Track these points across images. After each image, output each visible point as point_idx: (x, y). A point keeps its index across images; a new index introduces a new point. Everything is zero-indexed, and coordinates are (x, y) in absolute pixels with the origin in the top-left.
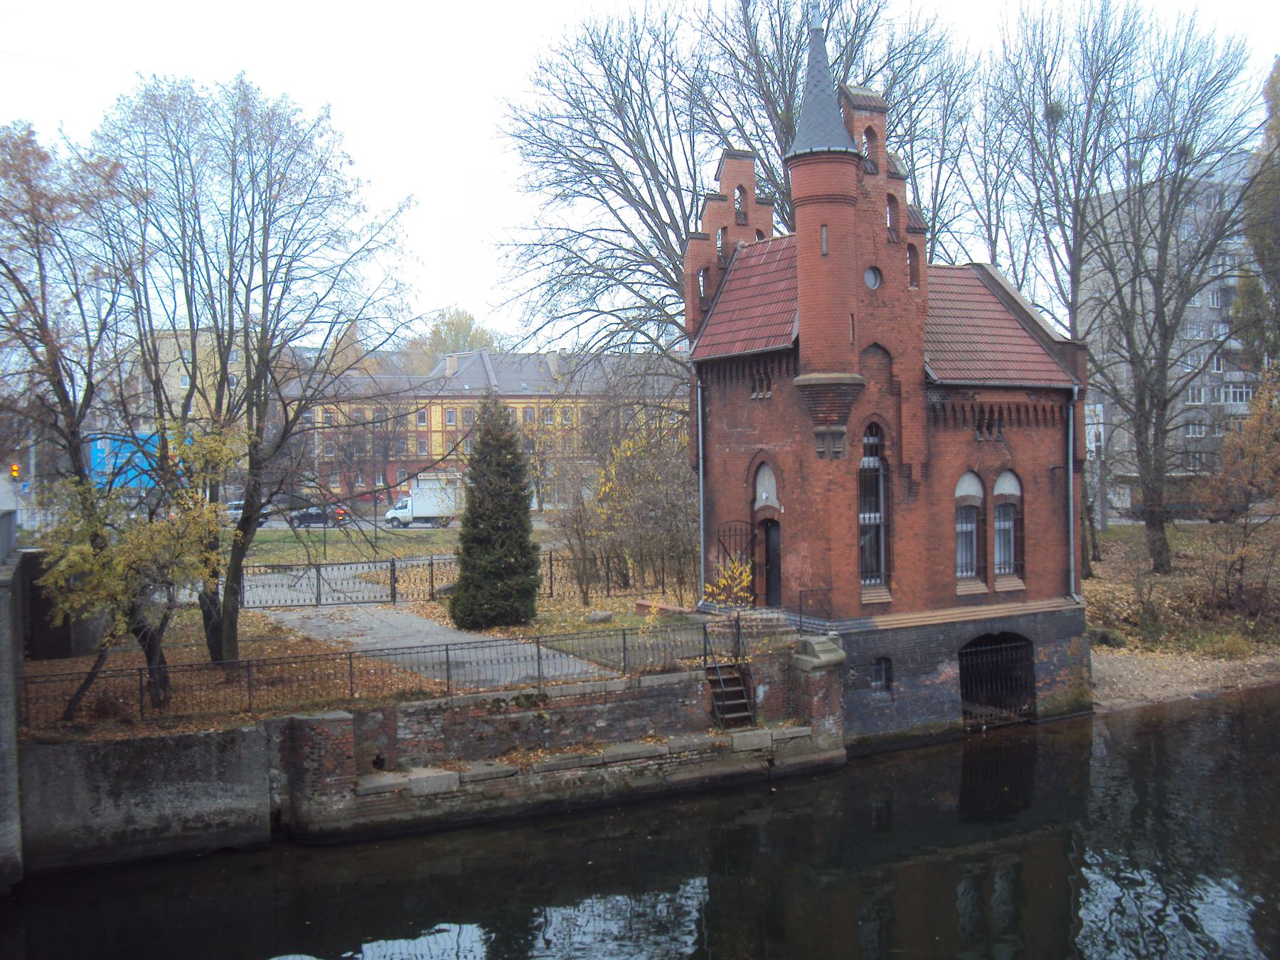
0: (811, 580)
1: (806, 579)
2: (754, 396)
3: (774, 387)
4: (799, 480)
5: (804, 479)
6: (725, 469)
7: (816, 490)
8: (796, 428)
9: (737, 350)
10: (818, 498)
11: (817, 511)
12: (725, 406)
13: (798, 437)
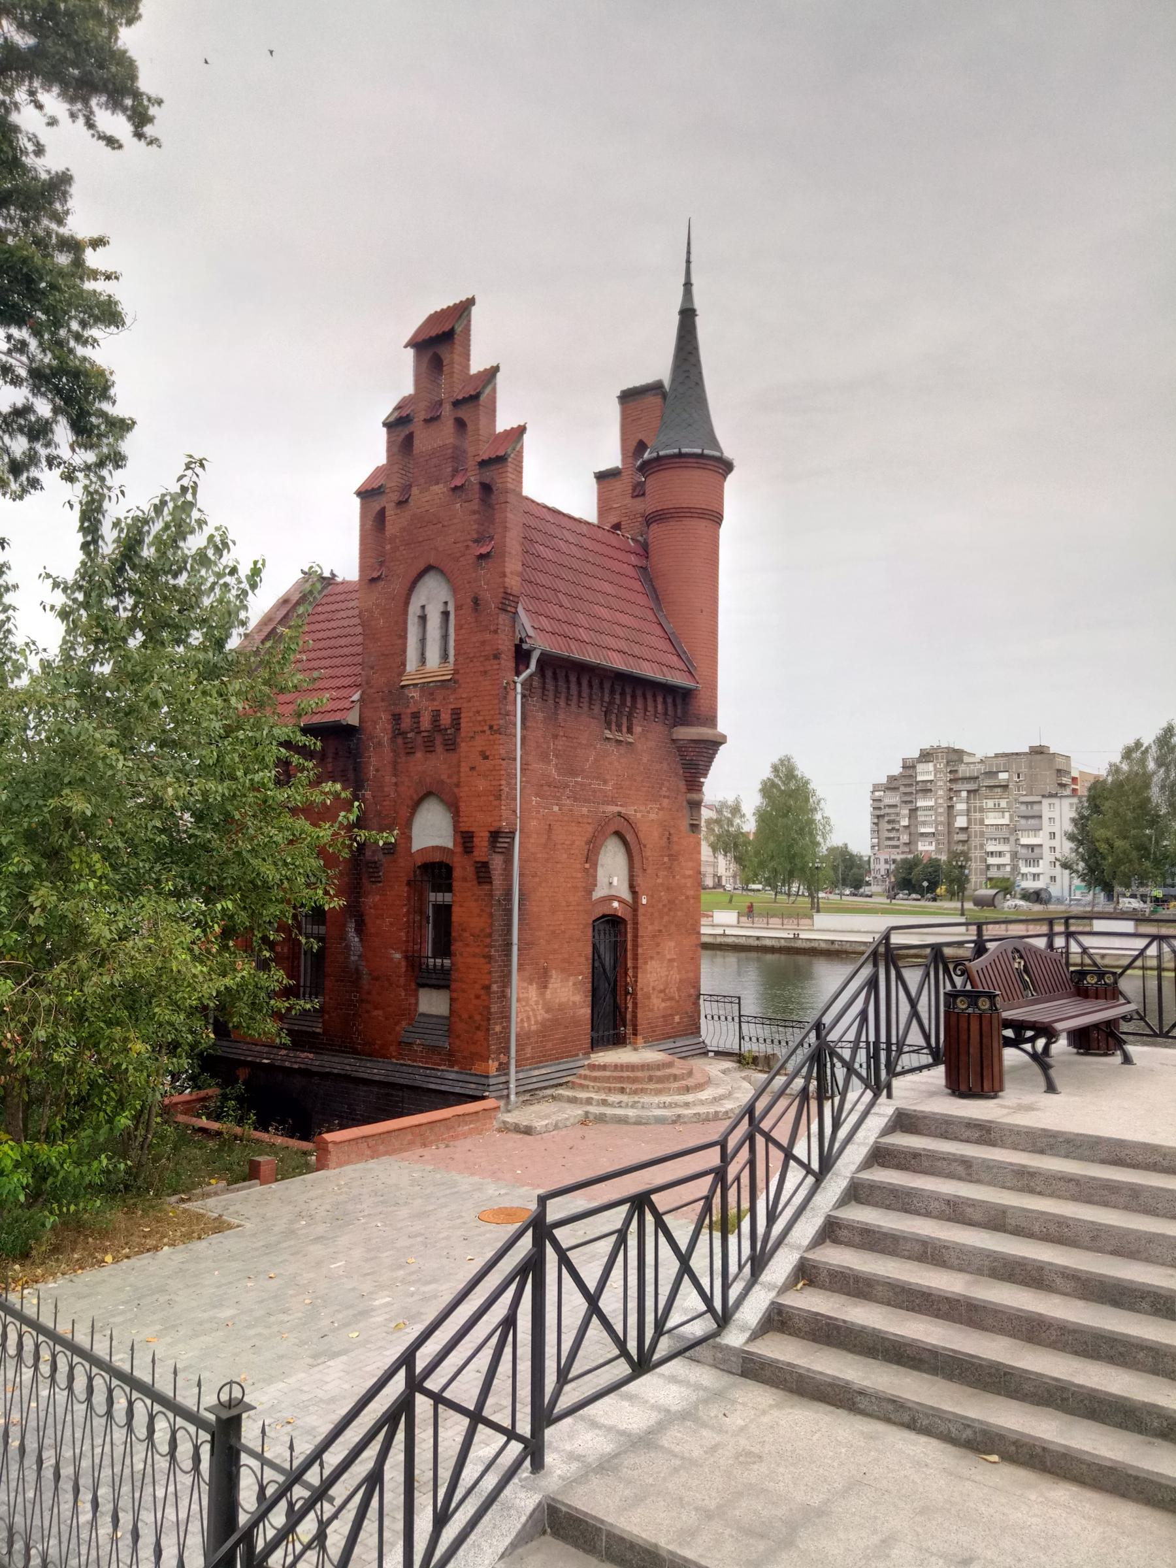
0: (679, 989)
1: (673, 991)
3: (638, 729)
4: (666, 859)
5: (673, 857)
6: (549, 838)
8: (664, 791)
9: (618, 663)
11: (687, 897)
12: (555, 737)
13: (666, 802)
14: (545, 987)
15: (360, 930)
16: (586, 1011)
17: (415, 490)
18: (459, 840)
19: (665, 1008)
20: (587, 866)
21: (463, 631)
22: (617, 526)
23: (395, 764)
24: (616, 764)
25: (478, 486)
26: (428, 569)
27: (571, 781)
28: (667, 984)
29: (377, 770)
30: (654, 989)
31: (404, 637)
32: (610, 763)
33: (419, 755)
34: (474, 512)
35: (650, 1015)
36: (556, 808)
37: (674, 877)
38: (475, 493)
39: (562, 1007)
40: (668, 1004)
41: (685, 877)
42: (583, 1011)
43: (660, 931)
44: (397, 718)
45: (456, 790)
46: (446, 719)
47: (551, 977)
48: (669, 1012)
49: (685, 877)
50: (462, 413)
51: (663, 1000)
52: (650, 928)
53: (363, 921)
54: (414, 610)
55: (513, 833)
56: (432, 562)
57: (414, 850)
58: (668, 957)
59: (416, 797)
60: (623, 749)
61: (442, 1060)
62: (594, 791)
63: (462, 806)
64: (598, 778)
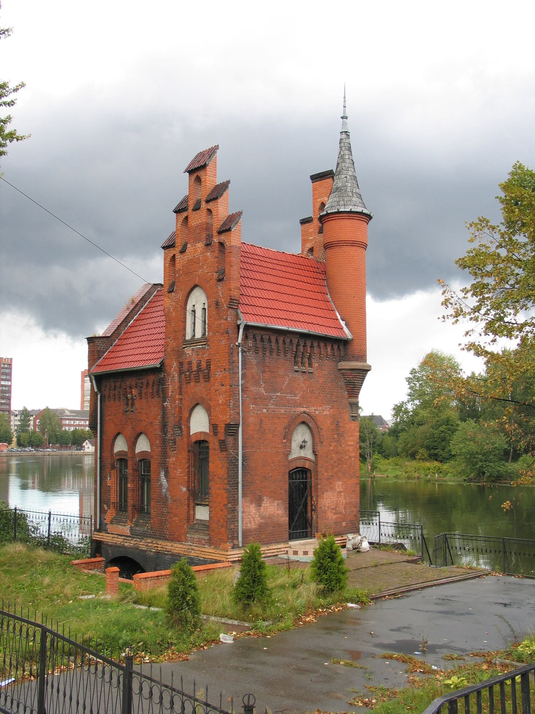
0: (345, 508)
1: (341, 509)
2: (296, 368)
3: (316, 365)
4: (336, 436)
5: (340, 435)
6: (261, 426)
7: (350, 443)
10: (351, 449)
11: (350, 457)
12: (264, 372)
14: (260, 506)
15: (166, 476)
16: (285, 519)
17: (189, 245)
18: (212, 429)
19: (337, 518)
20: (285, 441)
21: (211, 319)
22: (311, 250)
23: (180, 388)
24: (302, 385)
25: (218, 244)
26: (195, 286)
27: (274, 395)
28: (337, 506)
29: (172, 392)
30: (328, 508)
31: (185, 322)
32: (298, 385)
33: (192, 384)
34: (216, 257)
35: (326, 521)
36: (265, 411)
37: (341, 446)
38: (216, 248)
39: (270, 517)
40: (338, 516)
41: (349, 446)
42: (283, 518)
43: (332, 476)
44: (181, 364)
45: (209, 402)
46: (204, 364)
47: (263, 500)
48: (339, 520)
49: (349, 446)
50: (211, 205)
51: (335, 514)
52: (325, 474)
53: (168, 471)
54: (189, 307)
55: (239, 425)
56: (197, 282)
57: (191, 434)
58: (338, 490)
59: (191, 406)
60: (306, 376)
61: (206, 542)
62: (288, 400)
63: (212, 410)
64: (291, 393)
